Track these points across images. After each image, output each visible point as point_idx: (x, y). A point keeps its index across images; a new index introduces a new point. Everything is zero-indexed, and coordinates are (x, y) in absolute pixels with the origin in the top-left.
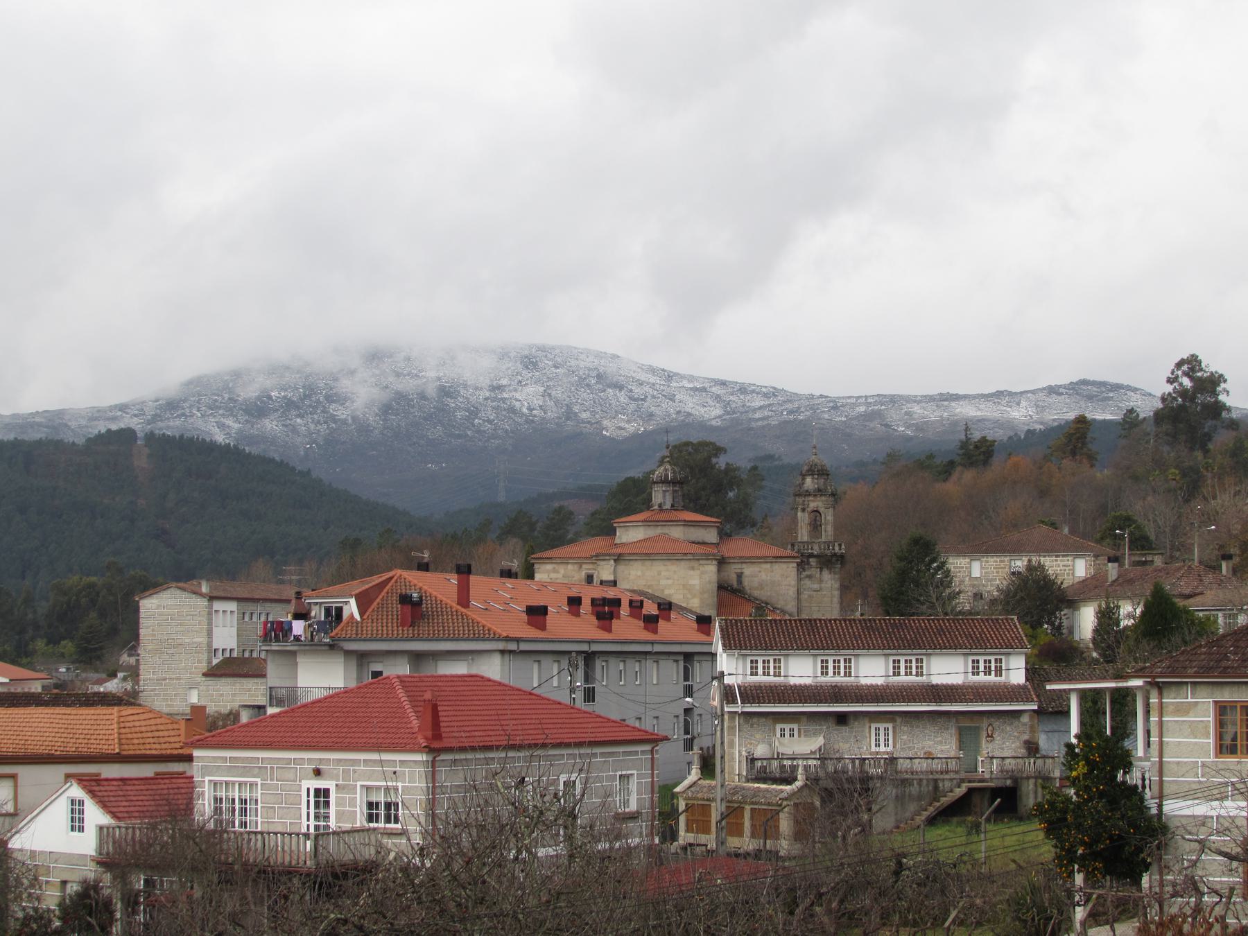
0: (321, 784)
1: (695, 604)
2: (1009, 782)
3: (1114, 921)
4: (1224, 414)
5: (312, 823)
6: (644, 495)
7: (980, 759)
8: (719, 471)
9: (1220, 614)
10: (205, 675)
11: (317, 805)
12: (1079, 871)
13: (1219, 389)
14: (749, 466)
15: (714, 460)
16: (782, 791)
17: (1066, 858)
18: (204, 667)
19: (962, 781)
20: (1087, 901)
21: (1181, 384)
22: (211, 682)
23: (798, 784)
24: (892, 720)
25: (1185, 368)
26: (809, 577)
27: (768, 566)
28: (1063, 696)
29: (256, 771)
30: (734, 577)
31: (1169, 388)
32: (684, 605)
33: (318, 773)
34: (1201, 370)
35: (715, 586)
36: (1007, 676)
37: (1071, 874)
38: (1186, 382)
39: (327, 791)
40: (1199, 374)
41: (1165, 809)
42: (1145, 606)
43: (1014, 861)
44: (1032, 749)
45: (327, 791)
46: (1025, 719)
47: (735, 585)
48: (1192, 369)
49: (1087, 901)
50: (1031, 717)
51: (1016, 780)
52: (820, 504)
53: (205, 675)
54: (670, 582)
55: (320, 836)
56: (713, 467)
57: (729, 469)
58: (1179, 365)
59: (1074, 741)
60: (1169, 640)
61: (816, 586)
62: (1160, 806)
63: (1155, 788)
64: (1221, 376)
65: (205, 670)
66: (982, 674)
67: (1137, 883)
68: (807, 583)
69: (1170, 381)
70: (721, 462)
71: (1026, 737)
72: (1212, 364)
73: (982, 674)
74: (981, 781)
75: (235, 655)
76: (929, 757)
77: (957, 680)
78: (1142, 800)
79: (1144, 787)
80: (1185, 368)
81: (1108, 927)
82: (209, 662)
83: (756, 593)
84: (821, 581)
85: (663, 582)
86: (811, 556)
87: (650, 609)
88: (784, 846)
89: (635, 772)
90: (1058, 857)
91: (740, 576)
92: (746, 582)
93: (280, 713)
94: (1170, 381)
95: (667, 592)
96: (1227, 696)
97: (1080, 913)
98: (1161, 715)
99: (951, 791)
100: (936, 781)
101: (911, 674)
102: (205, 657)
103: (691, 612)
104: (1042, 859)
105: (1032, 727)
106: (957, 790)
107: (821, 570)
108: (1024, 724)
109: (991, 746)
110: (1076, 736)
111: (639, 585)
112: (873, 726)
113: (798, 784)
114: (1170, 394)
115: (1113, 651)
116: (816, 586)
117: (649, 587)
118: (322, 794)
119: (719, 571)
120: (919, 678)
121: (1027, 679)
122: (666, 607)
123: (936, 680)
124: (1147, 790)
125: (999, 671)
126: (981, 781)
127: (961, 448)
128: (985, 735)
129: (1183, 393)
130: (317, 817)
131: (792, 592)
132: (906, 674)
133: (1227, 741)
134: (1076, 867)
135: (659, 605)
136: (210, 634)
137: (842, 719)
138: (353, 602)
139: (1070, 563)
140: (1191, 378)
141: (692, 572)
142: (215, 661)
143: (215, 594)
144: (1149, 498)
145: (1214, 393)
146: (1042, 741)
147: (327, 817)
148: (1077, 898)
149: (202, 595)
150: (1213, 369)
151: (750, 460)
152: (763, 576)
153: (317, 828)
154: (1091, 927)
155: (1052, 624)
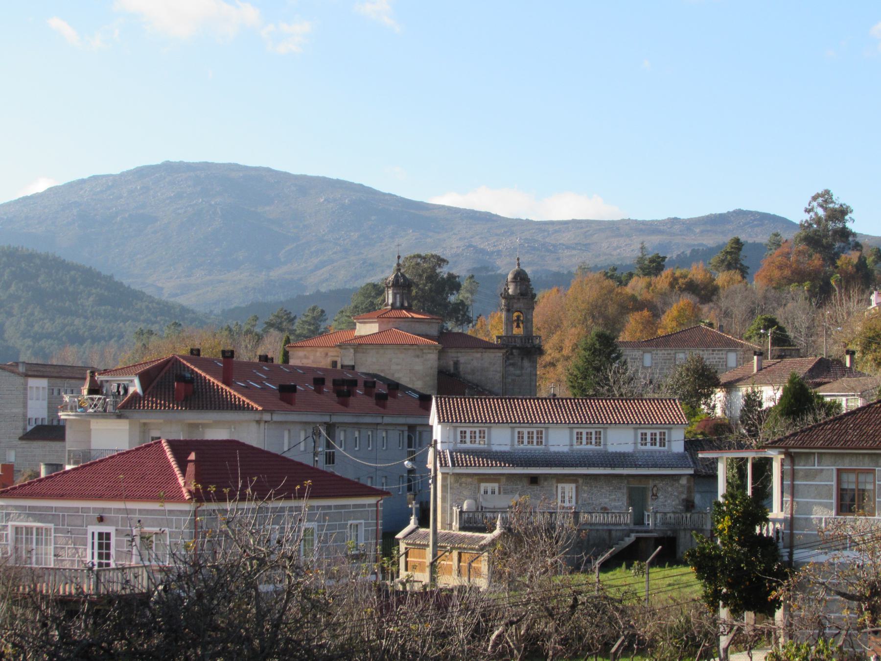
0: (104, 529)
1: (418, 385)
2: (669, 533)
3: (751, 649)
4: (851, 239)
5: (96, 560)
6: (382, 298)
7: (646, 513)
8: (443, 279)
9: (844, 399)
10: (21, 439)
11: (100, 546)
12: (724, 607)
13: (847, 217)
14: (468, 275)
15: (438, 270)
16: (483, 538)
17: (713, 600)
18: (20, 432)
19: (632, 531)
20: (730, 632)
21: (816, 214)
22: (25, 444)
23: (497, 532)
24: (575, 481)
25: (820, 200)
26: (513, 365)
27: (479, 355)
28: (713, 464)
29: (51, 517)
30: (451, 363)
31: (807, 217)
32: (410, 386)
33: (101, 519)
34: (832, 202)
35: (435, 372)
36: (670, 446)
37: (716, 609)
38: (821, 212)
39: (108, 535)
40: (831, 206)
41: (795, 557)
42: (784, 390)
43: (672, 599)
44: (689, 505)
45: (108, 535)
46: (684, 481)
47: (452, 370)
48: (825, 201)
49: (730, 632)
50: (688, 481)
51: (675, 531)
52: (522, 305)
53: (21, 439)
54: (399, 367)
55: (98, 573)
56: (437, 275)
57: (451, 277)
58: (815, 198)
59: (721, 500)
60: (802, 419)
61: (518, 372)
62: (791, 554)
63: (787, 540)
64: (848, 207)
65: (21, 435)
66: (648, 445)
67: (772, 615)
68: (511, 369)
69: (808, 211)
70: (443, 272)
71: (684, 496)
72: (840, 198)
73: (648, 445)
74: (646, 532)
75: (46, 423)
76: (605, 510)
77: (628, 448)
78: (776, 549)
79: (778, 538)
80: (820, 200)
81: (746, 652)
82: (25, 429)
83: (469, 377)
84: (522, 368)
85: (394, 367)
86: (515, 347)
87: (382, 389)
88: (482, 583)
89: (363, 521)
90: (706, 596)
91: (456, 364)
92: (461, 368)
93: (73, 469)
94: (808, 211)
95: (397, 375)
96: (846, 464)
97: (724, 641)
98: (793, 480)
99: (623, 540)
100: (610, 531)
101: (591, 443)
102: (21, 424)
103: (414, 391)
104: (695, 596)
105: (689, 488)
106: (627, 539)
107: (522, 359)
108: (683, 486)
109: (655, 503)
110: (724, 496)
111: (374, 369)
112: (560, 486)
113: (497, 532)
114: (806, 221)
115: (757, 428)
116: (518, 372)
117: (382, 371)
118: (104, 537)
119: (439, 359)
120: (598, 447)
121: (686, 449)
122: (394, 387)
123: (611, 449)
124: (780, 540)
125: (662, 444)
126: (646, 532)
127: (639, 262)
128: (650, 494)
129: (819, 221)
130: (100, 556)
131: (498, 376)
132: (652, 445)
133: (847, 501)
134: (721, 603)
135: (389, 385)
136: (25, 405)
137: (534, 480)
138: (137, 381)
139: (724, 356)
140: (825, 209)
141: (417, 360)
142: (29, 428)
143: (30, 373)
144: (789, 305)
145: (842, 220)
146: (697, 499)
147: (108, 556)
148: (721, 629)
149: (19, 374)
150: (841, 201)
151: (468, 271)
152: (475, 363)
153: (100, 565)
154: (732, 653)
155: (708, 405)
